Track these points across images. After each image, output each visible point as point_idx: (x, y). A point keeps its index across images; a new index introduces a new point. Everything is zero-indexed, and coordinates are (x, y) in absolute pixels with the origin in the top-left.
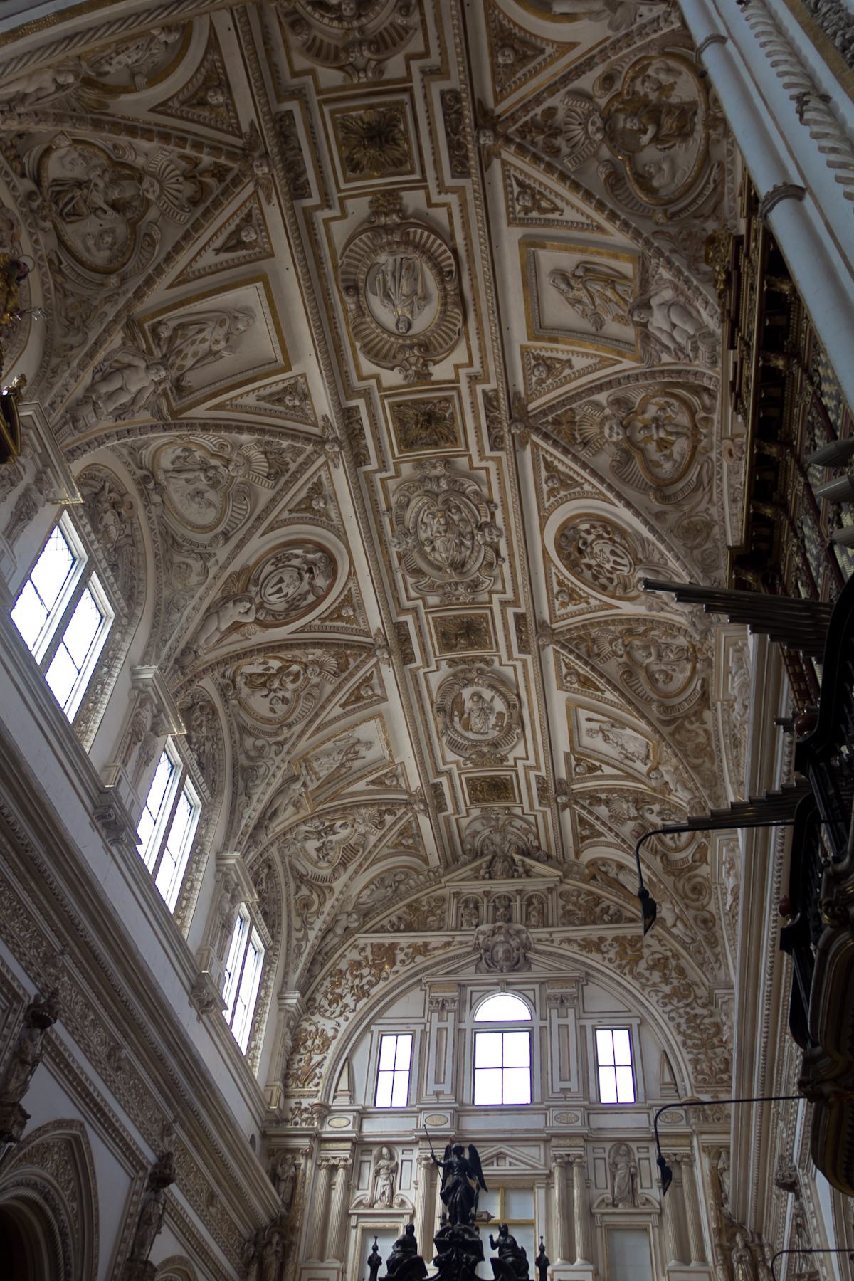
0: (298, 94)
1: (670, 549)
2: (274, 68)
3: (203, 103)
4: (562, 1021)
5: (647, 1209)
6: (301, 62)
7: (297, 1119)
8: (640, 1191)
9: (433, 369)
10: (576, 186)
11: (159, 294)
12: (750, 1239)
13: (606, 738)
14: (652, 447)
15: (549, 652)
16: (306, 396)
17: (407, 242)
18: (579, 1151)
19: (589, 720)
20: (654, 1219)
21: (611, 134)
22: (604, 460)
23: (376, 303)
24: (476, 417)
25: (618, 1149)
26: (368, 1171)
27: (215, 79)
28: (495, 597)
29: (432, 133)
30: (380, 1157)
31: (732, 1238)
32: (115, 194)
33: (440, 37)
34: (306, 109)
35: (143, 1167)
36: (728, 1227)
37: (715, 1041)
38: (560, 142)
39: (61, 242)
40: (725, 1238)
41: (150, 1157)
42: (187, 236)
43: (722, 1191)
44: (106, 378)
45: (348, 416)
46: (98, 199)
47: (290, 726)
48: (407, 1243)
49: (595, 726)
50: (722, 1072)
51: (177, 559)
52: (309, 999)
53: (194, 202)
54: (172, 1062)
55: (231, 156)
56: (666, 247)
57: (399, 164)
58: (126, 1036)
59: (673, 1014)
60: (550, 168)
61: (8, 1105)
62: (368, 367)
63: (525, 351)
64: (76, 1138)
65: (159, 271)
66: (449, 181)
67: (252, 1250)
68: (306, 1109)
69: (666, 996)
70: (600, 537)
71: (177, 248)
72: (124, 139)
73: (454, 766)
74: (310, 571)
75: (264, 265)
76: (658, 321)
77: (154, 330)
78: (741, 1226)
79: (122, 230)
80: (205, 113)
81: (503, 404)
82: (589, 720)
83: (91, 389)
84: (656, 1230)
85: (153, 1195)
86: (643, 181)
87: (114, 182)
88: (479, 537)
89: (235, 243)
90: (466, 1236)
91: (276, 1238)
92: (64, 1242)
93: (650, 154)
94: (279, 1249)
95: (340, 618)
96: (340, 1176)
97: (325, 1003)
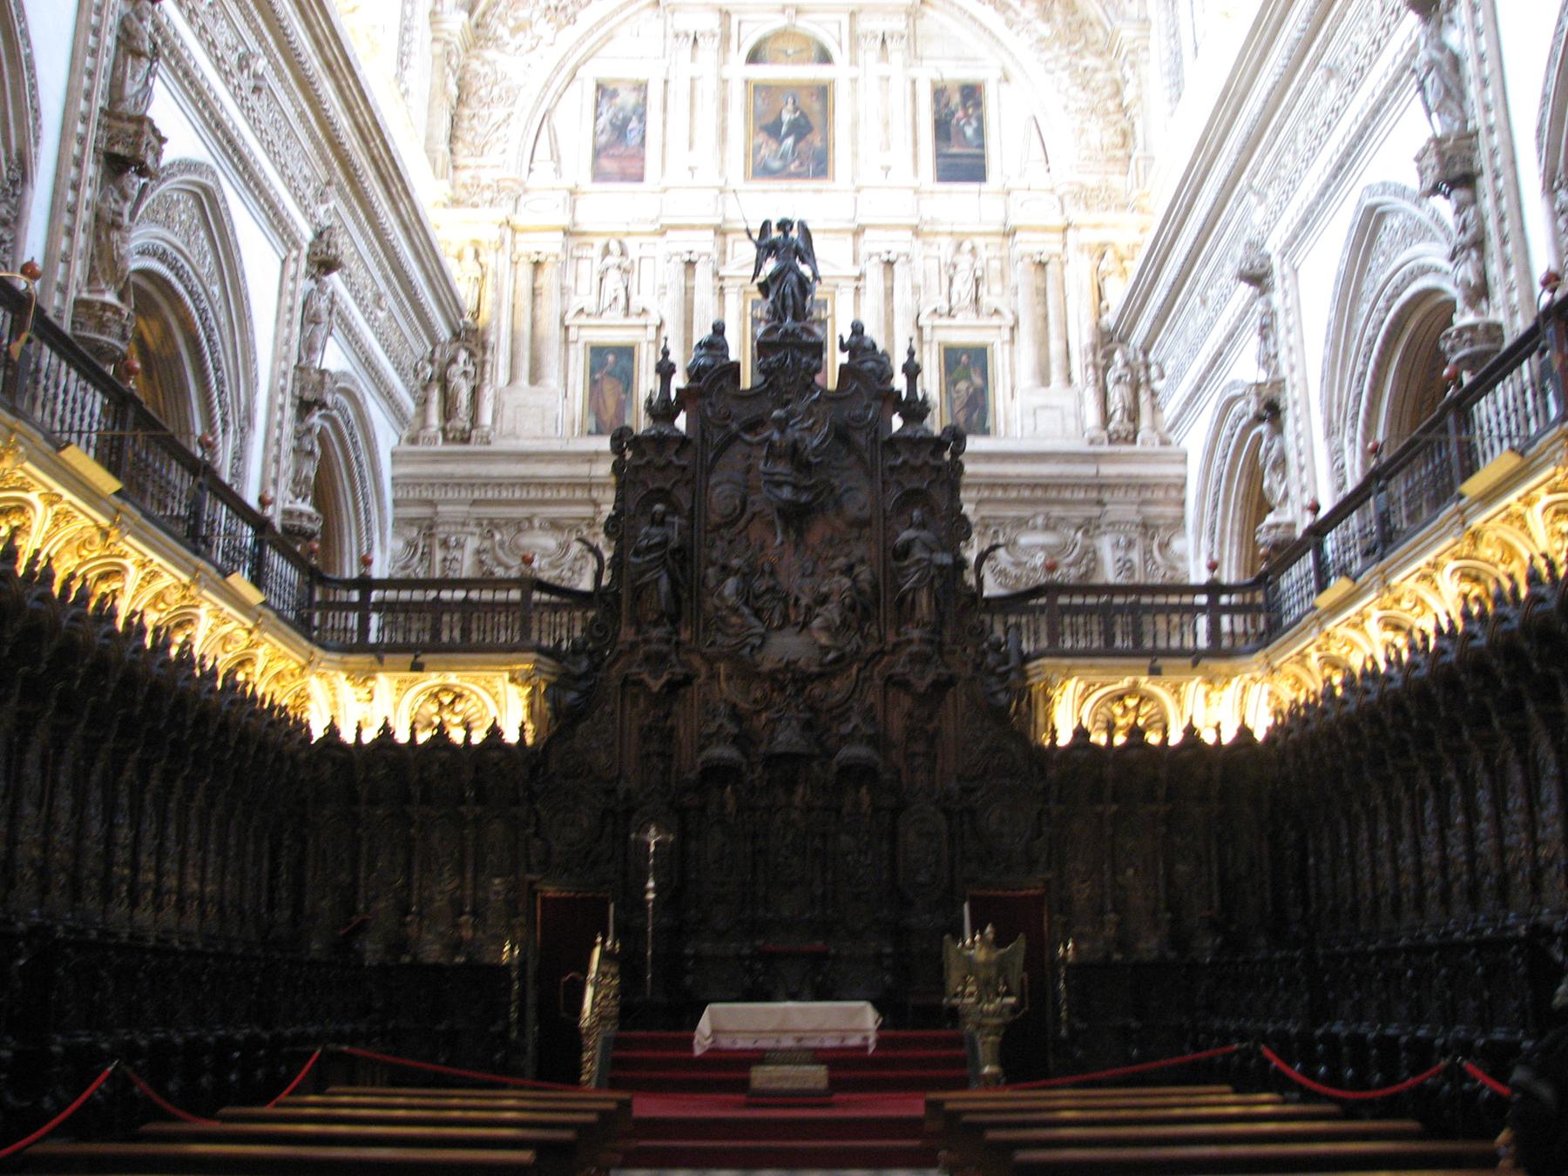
4: (884, 69)
5: (996, 321)
7: (475, 199)
8: (985, 299)
12: (1131, 356)
18: (904, 248)
20: (1006, 334)
25: (959, 245)
26: (587, 271)
30: (606, 251)
31: (1109, 355)
35: (296, 245)
36: (1107, 341)
37: (1111, 105)
40: (1100, 354)
41: (307, 233)
43: (1101, 299)
48: (716, 342)
50: (1115, 146)
52: (478, 26)
54: (327, 88)
58: (261, 39)
59: (1051, 66)
61: (131, 119)
64: (205, 188)
67: (429, 370)
68: (489, 187)
69: (1041, 40)
78: (1124, 340)
84: (1007, 347)
85: (312, 284)
90: (805, 337)
91: (463, 355)
92: (209, 340)
94: (470, 368)
96: (547, 278)
97: (503, 32)
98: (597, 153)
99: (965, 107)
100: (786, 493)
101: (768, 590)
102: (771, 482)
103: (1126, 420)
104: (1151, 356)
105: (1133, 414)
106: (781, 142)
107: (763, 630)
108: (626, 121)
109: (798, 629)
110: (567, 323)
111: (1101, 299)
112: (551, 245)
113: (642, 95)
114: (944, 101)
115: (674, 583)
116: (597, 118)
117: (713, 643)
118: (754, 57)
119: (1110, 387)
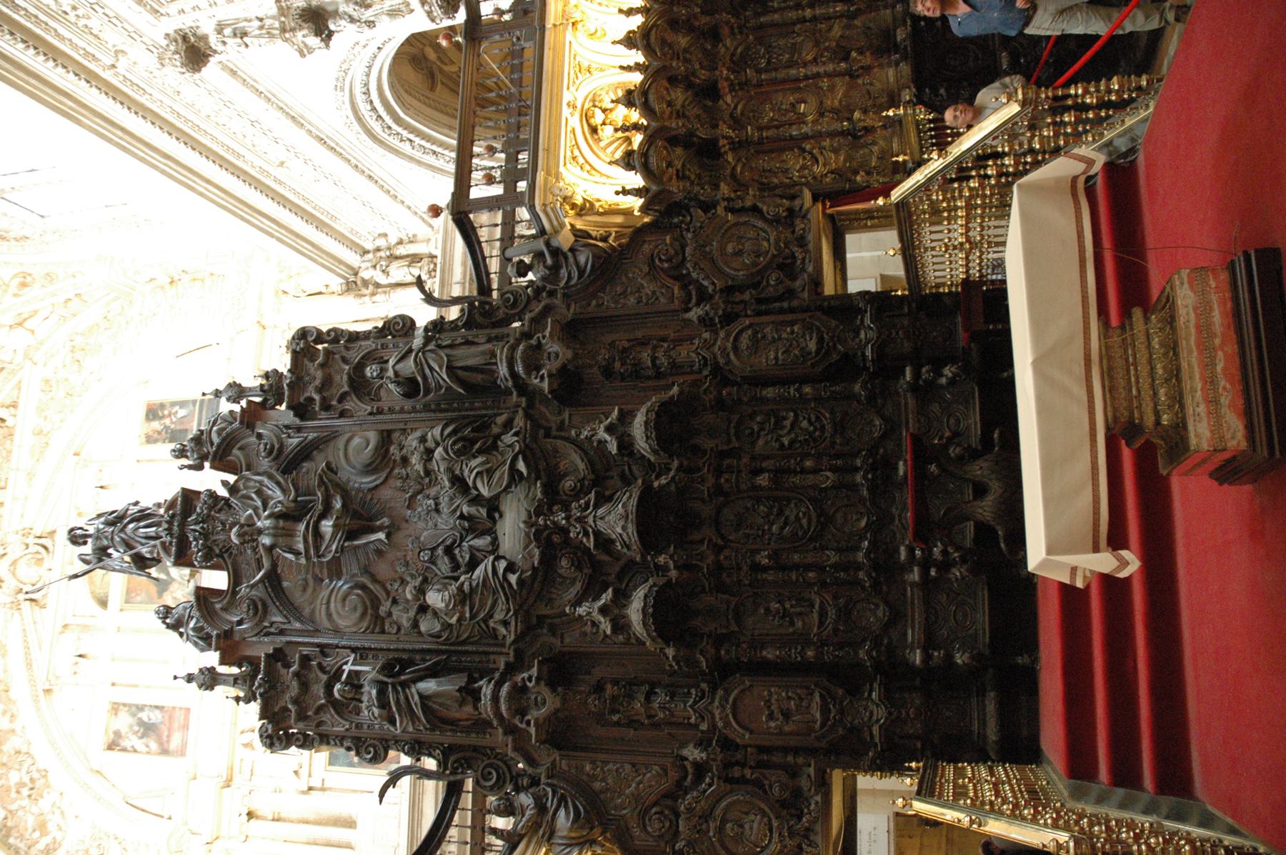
31: (366, 283)
40: (364, 291)
43: (320, 293)
98: (165, 751)
99: (163, 417)
100: (327, 526)
101: (449, 551)
102: (317, 548)
103: (419, 264)
104: (369, 246)
105: (415, 259)
106: (173, 580)
107: (491, 558)
108: (141, 723)
109: (497, 515)
110: (306, 789)
111: (320, 293)
112: (236, 802)
113: (121, 707)
114: (156, 435)
115: (433, 673)
116: (135, 751)
117: (505, 623)
118: (103, 603)
119: (392, 280)
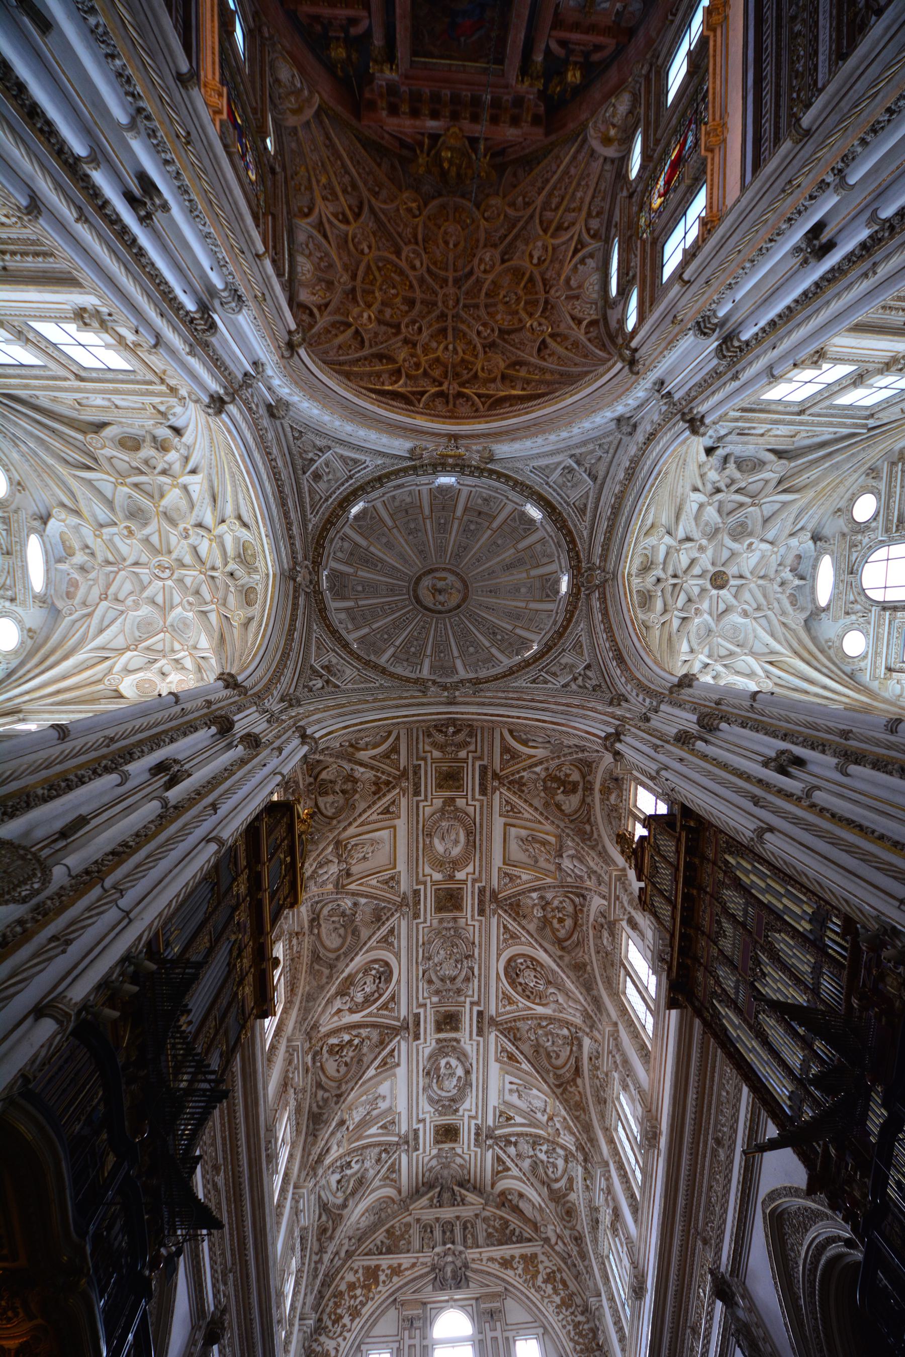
0: (425, 759)
1: (568, 977)
2: (417, 749)
3: (388, 757)
6: (427, 748)
9: (456, 873)
10: (531, 805)
11: (352, 830)
13: (520, 1096)
14: (555, 921)
15: (492, 1037)
16: (398, 883)
17: (456, 818)
19: (511, 1083)
21: (545, 789)
22: (532, 927)
23: (436, 841)
24: (473, 899)
27: (395, 749)
28: (468, 1000)
29: (473, 778)
32: (345, 787)
33: (482, 747)
34: (426, 764)
38: (524, 788)
39: (316, 805)
42: (369, 807)
44: (321, 866)
45: (416, 892)
46: (337, 788)
47: (346, 1083)
49: (514, 1087)
51: (317, 967)
53: (374, 793)
55: (394, 778)
56: (571, 833)
57: (459, 788)
60: (520, 797)
62: (428, 870)
63: (500, 868)
65: (355, 820)
66: (477, 796)
70: (528, 967)
71: (365, 811)
72: (356, 767)
73: (427, 1116)
74: (380, 978)
75: (396, 822)
76: (567, 864)
77: (346, 845)
79: (342, 801)
80: (388, 761)
81: (488, 894)
82: (511, 1083)
83: (314, 872)
86: (558, 806)
87: (344, 783)
88: (465, 963)
89: (386, 811)
93: (560, 797)
95: (387, 1009)
